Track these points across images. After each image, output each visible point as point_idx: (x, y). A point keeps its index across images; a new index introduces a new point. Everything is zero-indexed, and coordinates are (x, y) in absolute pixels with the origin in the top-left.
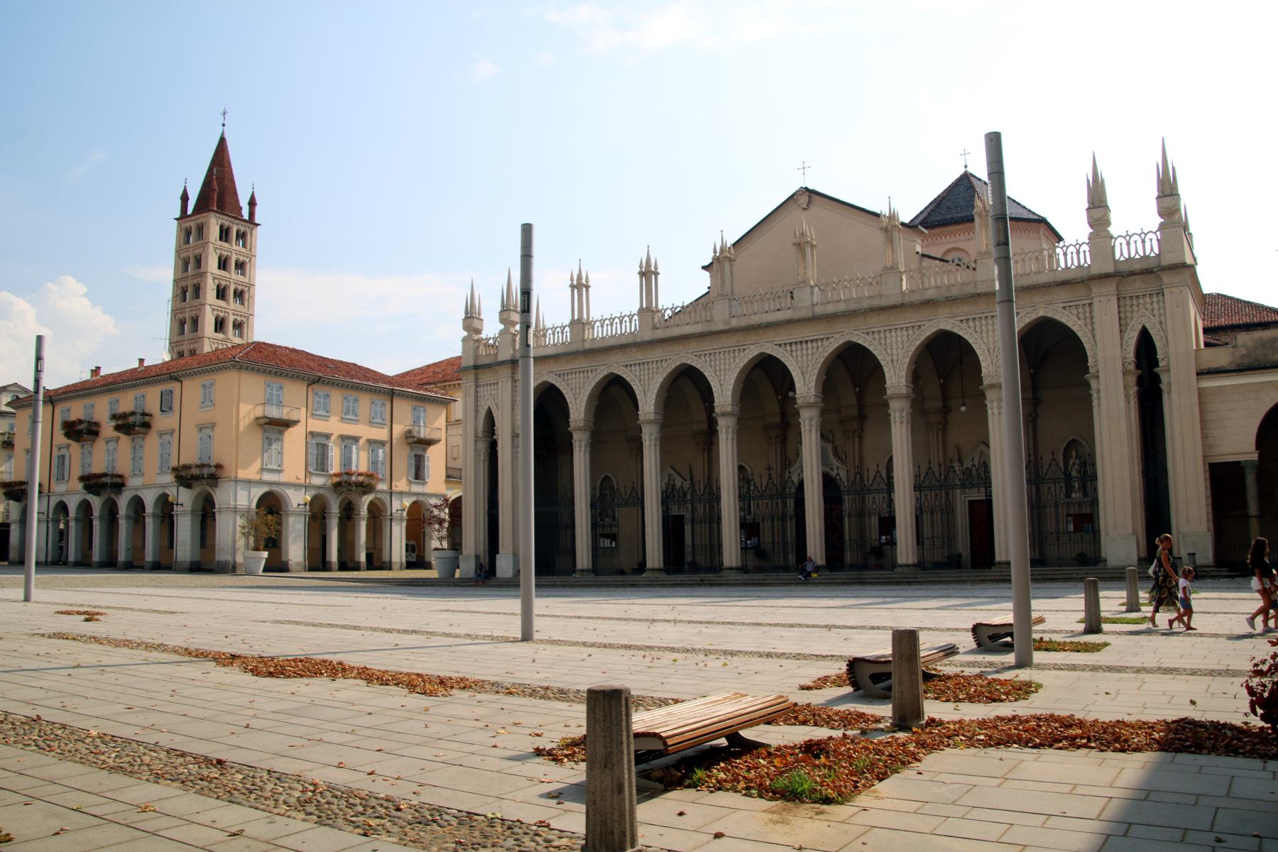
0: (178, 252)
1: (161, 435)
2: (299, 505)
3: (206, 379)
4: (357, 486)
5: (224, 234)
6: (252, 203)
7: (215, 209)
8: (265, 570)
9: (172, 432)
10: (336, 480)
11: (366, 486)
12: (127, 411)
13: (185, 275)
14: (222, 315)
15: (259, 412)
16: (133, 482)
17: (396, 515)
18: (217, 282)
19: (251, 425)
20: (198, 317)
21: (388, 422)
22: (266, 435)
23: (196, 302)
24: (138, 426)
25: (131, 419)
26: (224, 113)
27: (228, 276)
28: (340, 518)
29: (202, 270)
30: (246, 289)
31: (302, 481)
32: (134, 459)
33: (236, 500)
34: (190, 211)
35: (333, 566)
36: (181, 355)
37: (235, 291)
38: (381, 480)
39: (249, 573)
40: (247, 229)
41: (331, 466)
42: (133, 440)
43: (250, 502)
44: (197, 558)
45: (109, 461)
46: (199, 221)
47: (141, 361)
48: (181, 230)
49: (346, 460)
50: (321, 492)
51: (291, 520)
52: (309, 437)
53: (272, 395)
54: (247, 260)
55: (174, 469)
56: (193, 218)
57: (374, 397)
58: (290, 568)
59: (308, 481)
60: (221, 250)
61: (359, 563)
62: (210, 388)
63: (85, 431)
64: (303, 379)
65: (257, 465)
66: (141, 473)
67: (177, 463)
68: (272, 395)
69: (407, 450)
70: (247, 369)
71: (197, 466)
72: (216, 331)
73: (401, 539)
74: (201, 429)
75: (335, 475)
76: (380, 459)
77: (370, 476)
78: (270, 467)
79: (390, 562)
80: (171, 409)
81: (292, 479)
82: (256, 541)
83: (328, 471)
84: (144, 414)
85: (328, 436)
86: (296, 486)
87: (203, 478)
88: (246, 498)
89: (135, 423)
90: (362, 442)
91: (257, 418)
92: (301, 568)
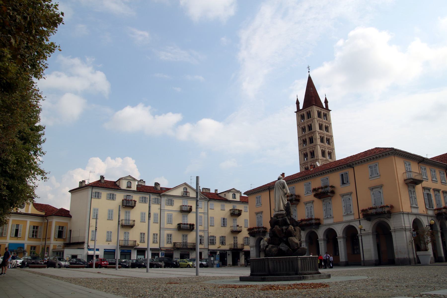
0: (298, 125)
3: (372, 164)
5: (319, 114)
6: (326, 102)
7: (315, 104)
10: (436, 211)
16: (326, 222)
20: (313, 151)
23: (312, 145)
24: (329, 193)
27: (323, 132)
30: (330, 138)
34: (301, 107)
36: (307, 169)
37: (327, 138)
40: (327, 112)
45: (308, 213)
46: (308, 111)
48: (299, 116)
49: (438, 203)
54: (329, 126)
60: (319, 121)
63: (294, 200)
66: (331, 217)
80: (348, 182)
83: (433, 208)
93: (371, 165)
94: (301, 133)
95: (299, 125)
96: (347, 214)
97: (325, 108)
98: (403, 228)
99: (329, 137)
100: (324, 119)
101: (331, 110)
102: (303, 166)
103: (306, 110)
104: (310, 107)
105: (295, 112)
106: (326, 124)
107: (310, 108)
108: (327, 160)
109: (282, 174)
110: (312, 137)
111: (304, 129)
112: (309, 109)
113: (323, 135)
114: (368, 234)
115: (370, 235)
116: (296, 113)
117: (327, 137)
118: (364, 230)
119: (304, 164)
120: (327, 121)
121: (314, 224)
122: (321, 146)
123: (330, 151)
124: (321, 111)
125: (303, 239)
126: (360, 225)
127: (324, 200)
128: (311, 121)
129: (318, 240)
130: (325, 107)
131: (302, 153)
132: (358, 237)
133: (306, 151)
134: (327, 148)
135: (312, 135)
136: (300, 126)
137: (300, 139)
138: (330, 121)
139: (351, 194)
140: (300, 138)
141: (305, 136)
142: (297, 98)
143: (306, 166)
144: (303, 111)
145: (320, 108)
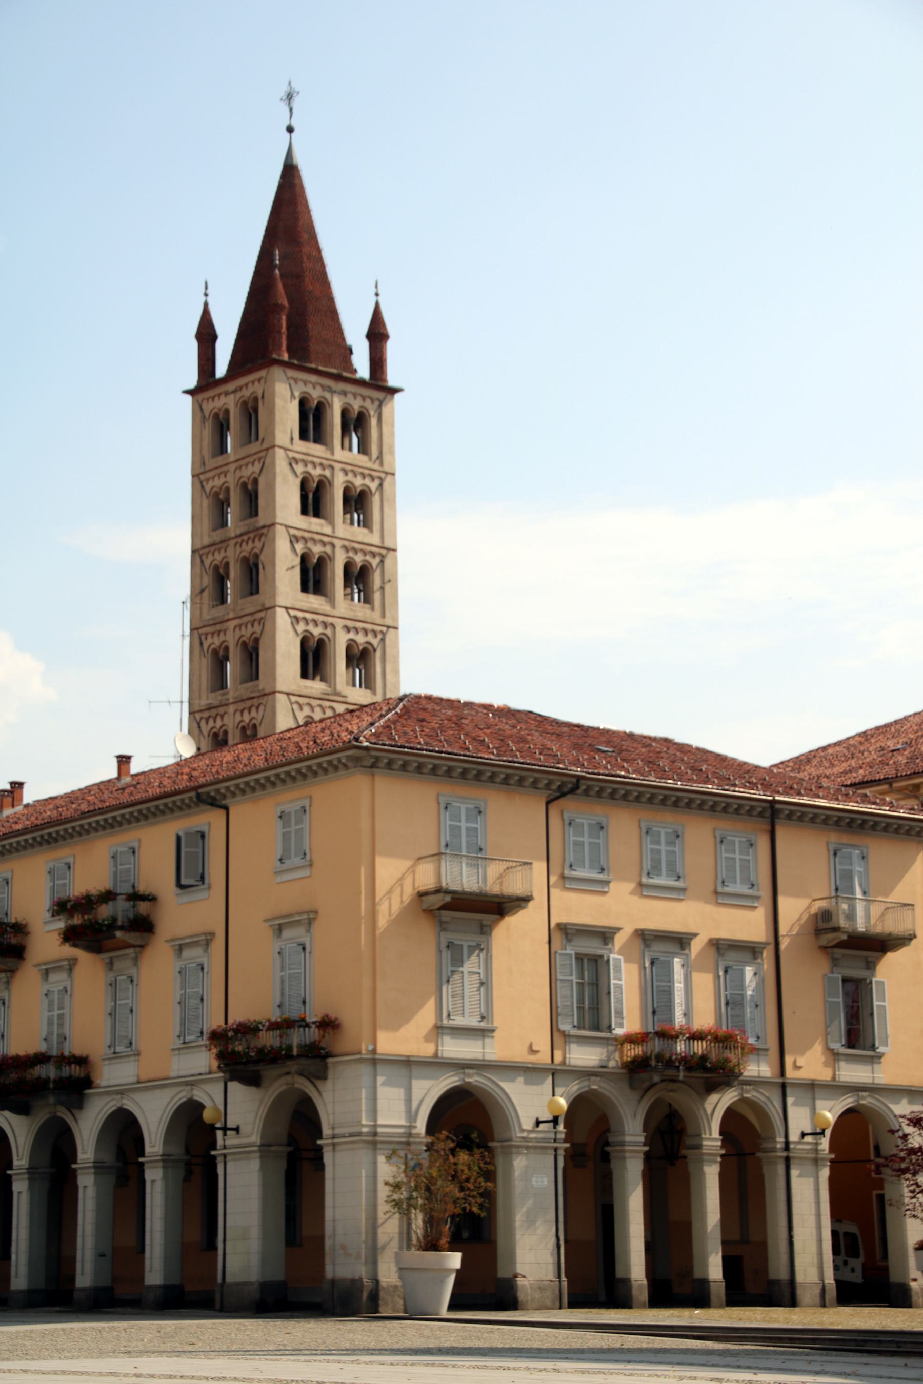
0: (199, 476)
1: (180, 949)
2: (538, 1123)
4: (689, 1069)
7: (285, 357)
8: (454, 1306)
9: (207, 940)
10: (632, 1052)
11: (715, 1069)
12: (94, 892)
13: (218, 536)
14: (317, 631)
15: (426, 877)
17: (800, 1148)
18: (299, 547)
19: (405, 912)
20: (257, 640)
21: (765, 891)
22: (445, 937)
23: (250, 604)
24: (122, 928)
25: (104, 911)
26: (290, 97)
27: (327, 530)
28: (648, 1158)
29: (262, 520)
30: (375, 562)
31: (543, 1057)
32: (112, 1014)
33: (374, 1112)
34: (221, 369)
35: (635, 1292)
36: (219, 741)
37: (348, 567)
38: (754, 1050)
39: (413, 1313)
41: (619, 1014)
42: (110, 965)
43: (412, 1116)
44: (278, 1275)
45: (50, 1023)
46: (246, 393)
47: (124, 761)
50: (595, 1085)
51: (519, 1163)
52: (557, 938)
53: (455, 831)
54: (373, 486)
55: (216, 1036)
56: (231, 386)
57: (724, 825)
58: (521, 1296)
59: (558, 1057)
60: (305, 464)
61: (704, 1283)
62: (298, 822)
64: (535, 784)
65: (426, 1017)
67: (221, 1022)
68: (455, 831)
69: (822, 966)
70: (389, 765)
71: (274, 1026)
72: (304, 675)
73: (818, 1215)
74: (280, 929)
75: (630, 1039)
76: (749, 993)
77: (723, 1040)
78: (459, 1021)
79: (792, 1282)
80: (202, 878)
81: (517, 1054)
82: (430, 1221)
83: (609, 1029)
84: (135, 897)
85: (606, 935)
86: (530, 1072)
87: (289, 1056)
88: (401, 1107)
89: (114, 919)
90: (696, 946)
91: (422, 895)
92: (550, 1296)
93: (287, 808)
94: (206, 524)
95: (202, 477)
96: (184, 1043)
98: (359, 1134)
102: (203, 723)
103: (241, 388)
105: (187, 392)
106: (350, 477)
107: (259, 380)
108: (339, 694)
109: (8, 787)
112: (253, 382)
113: (324, 544)
116: (189, 398)
117: (351, 554)
118: (237, 1130)
119: (206, 714)
120: (363, 460)
121: (51, 1086)
122: (300, 614)
123: (361, 639)
124: (327, 395)
125: (21, 1159)
127: (111, 958)
128: (257, 463)
129: (10, 1176)
131: (205, 648)
133: (222, 638)
134: (339, 623)
135: (258, 544)
136: (208, 480)
137: (198, 561)
138: (386, 458)
140: (201, 556)
141: (224, 545)
142: (206, 305)
143: (219, 723)
144: (227, 394)
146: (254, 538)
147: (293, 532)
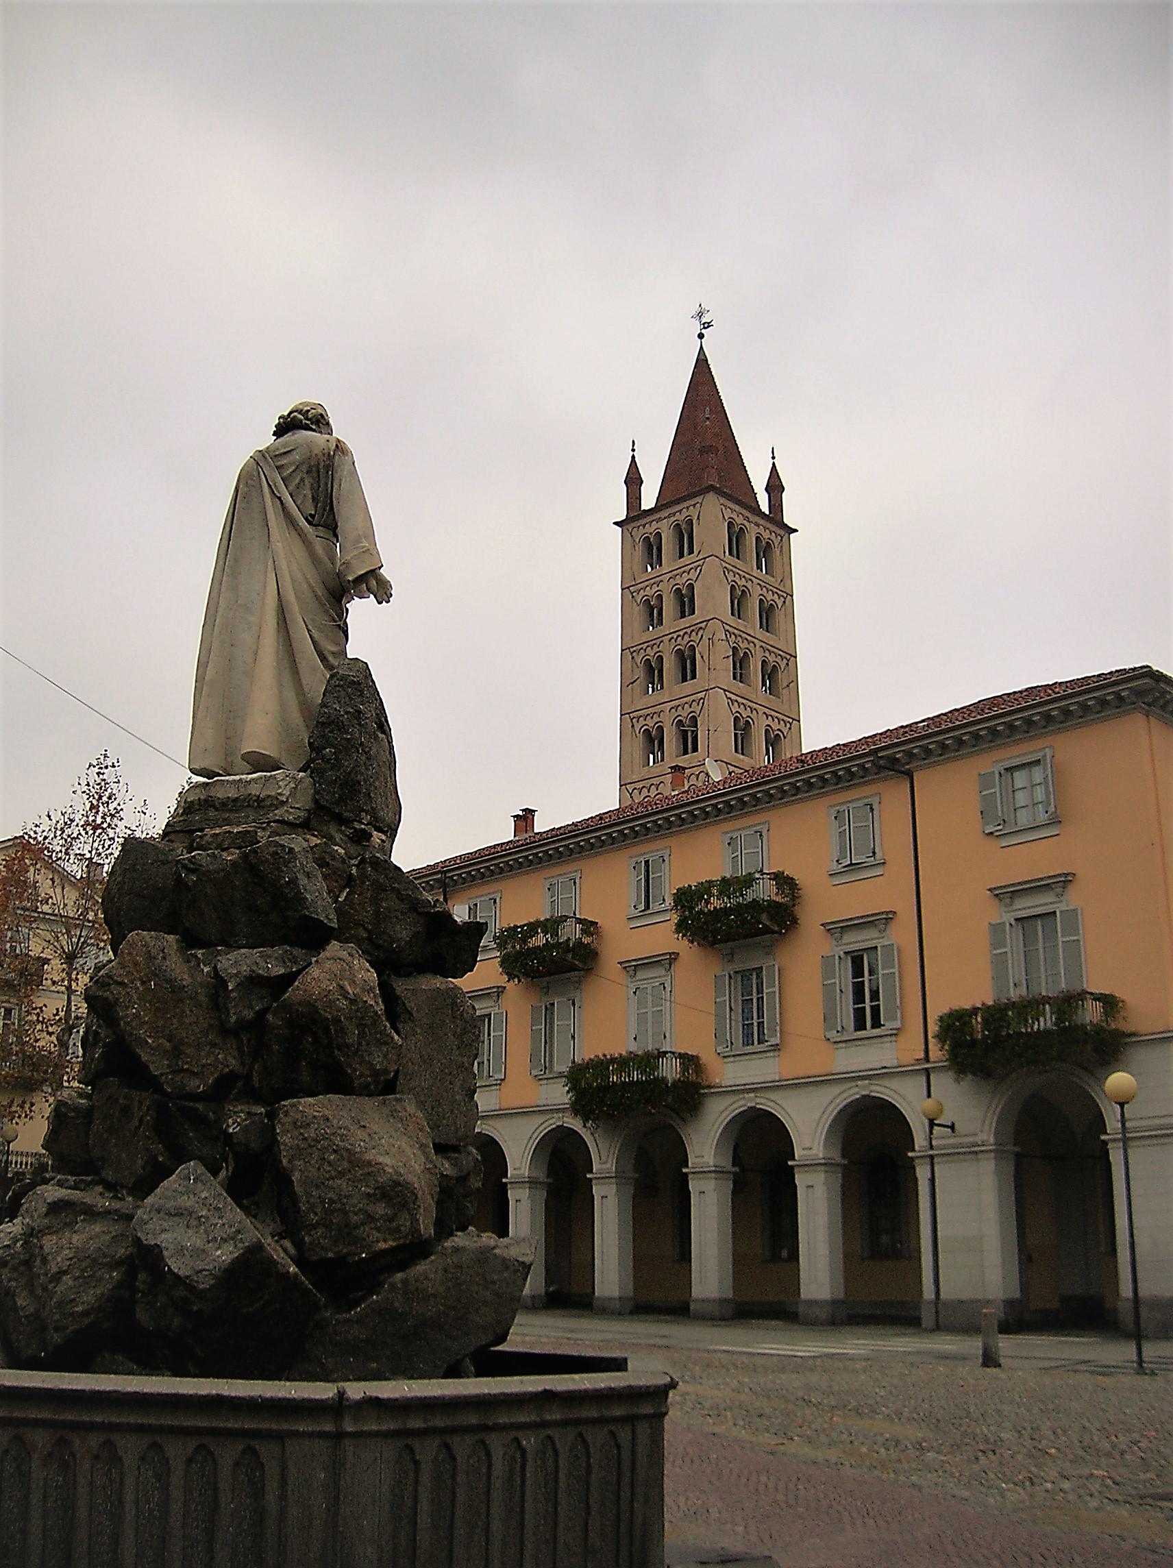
5: (736, 539)
6: (775, 486)
20: (694, 721)
34: (649, 499)
97: (767, 512)
99: (778, 659)
100: (759, 567)
101: (796, 531)
104: (692, 502)
105: (616, 523)
107: (694, 505)
109: (521, 813)
110: (693, 648)
111: (653, 612)
112: (688, 508)
114: (973, 1153)
115: (980, 1156)
116: (620, 529)
118: (952, 1127)
120: (770, 579)
122: (733, 697)
126: (929, 1096)
130: (765, 508)
132: (914, 1168)
133: (656, 719)
139: (885, 919)
143: (653, 792)
145: (744, 511)
146: (691, 632)
147: (727, 627)
